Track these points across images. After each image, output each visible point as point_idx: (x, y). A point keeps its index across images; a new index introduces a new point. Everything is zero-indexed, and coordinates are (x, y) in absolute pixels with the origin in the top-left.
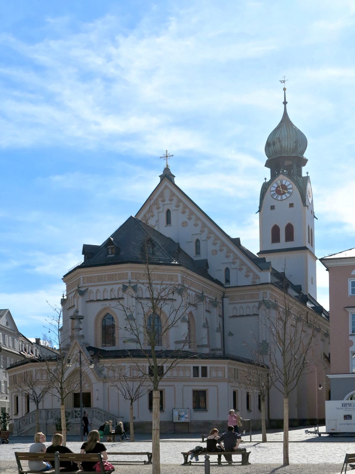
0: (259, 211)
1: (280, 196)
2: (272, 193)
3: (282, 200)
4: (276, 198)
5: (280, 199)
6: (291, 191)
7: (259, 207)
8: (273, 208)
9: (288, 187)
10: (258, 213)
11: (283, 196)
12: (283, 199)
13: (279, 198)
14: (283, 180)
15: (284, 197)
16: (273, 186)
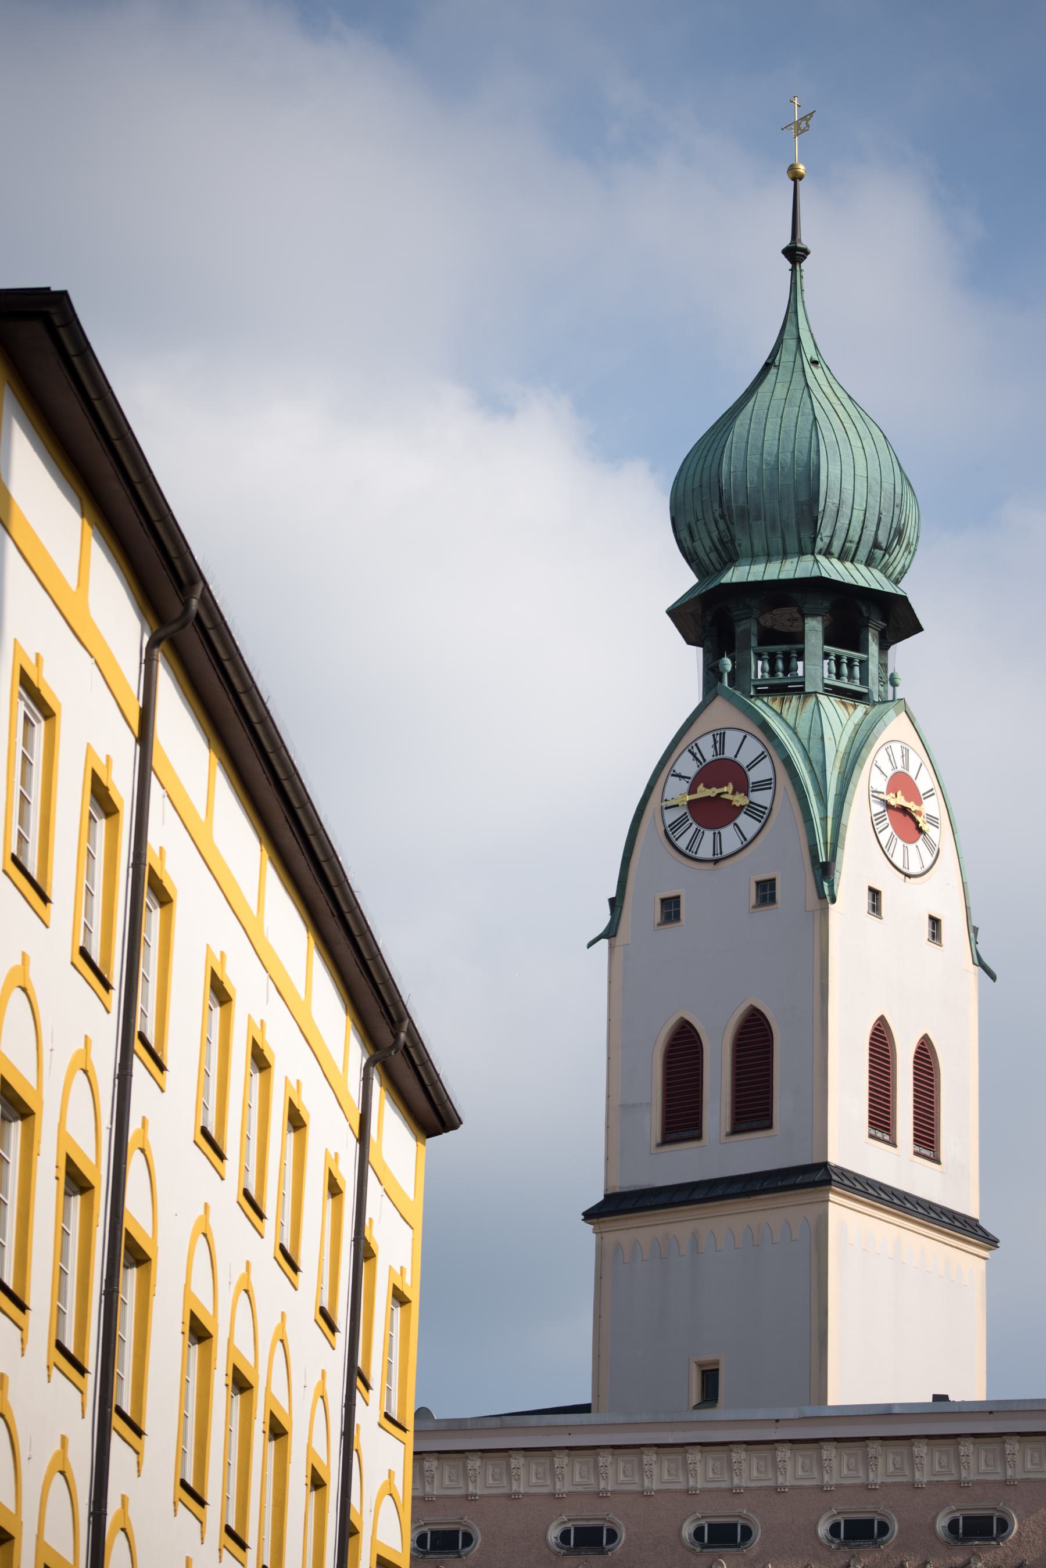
0: (610, 933)
1: (709, 834)
2: (671, 816)
3: (716, 862)
4: (689, 846)
5: (709, 855)
6: (762, 798)
7: (616, 904)
8: (671, 909)
9: (754, 776)
10: (604, 942)
11: (723, 831)
12: (725, 853)
13: (705, 850)
14: (728, 732)
15: (730, 837)
16: (678, 769)
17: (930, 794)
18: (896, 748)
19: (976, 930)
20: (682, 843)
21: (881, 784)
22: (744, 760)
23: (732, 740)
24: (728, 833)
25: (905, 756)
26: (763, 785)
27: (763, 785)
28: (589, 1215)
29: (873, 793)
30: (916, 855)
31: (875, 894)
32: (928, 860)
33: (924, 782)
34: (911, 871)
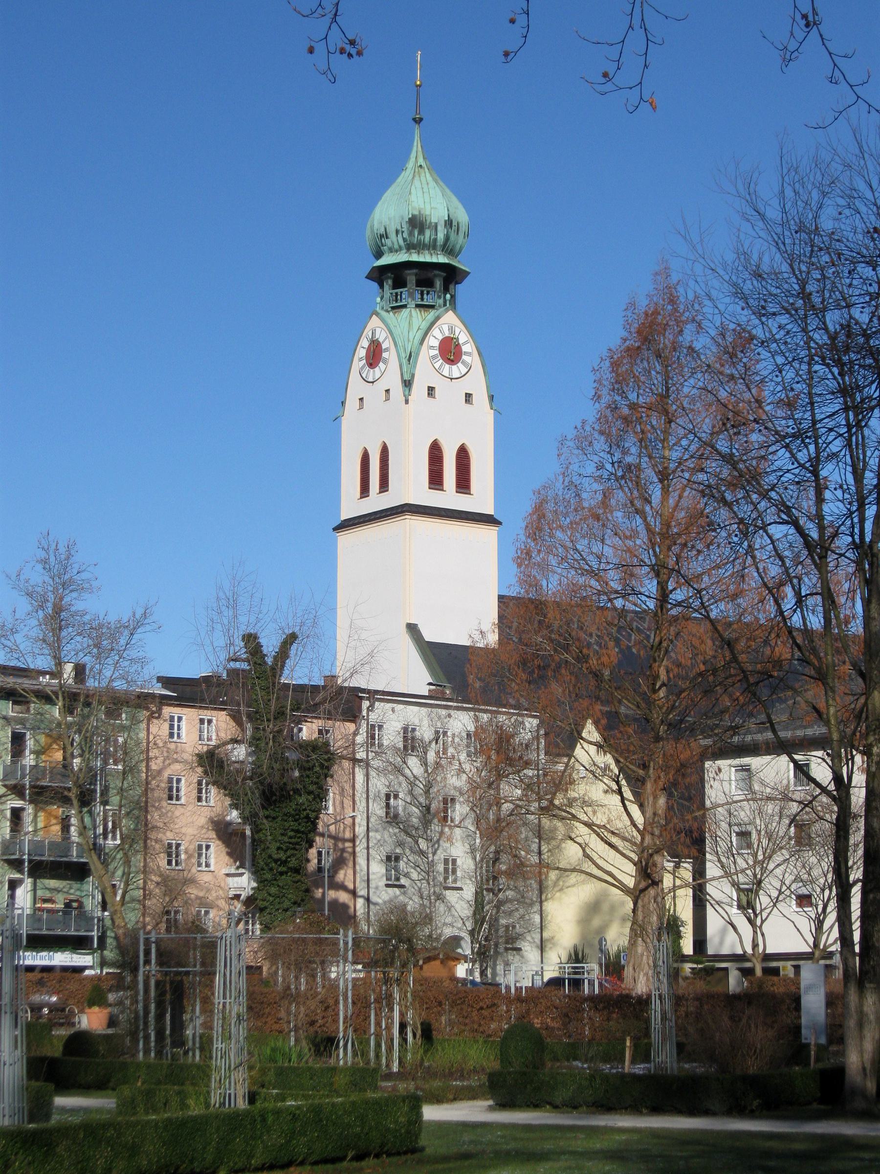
3: (373, 382)
17: (466, 343)
18: (445, 328)
19: (493, 396)
20: (364, 376)
21: (436, 343)
22: (381, 340)
23: (378, 331)
24: (377, 369)
25: (451, 329)
26: (387, 350)
27: (387, 350)
28: (335, 529)
29: (432, 347)
30: (457, 370)
31: (431, 391)
32: (464, 370)
33: (463, 337)
34: (454, 376)
